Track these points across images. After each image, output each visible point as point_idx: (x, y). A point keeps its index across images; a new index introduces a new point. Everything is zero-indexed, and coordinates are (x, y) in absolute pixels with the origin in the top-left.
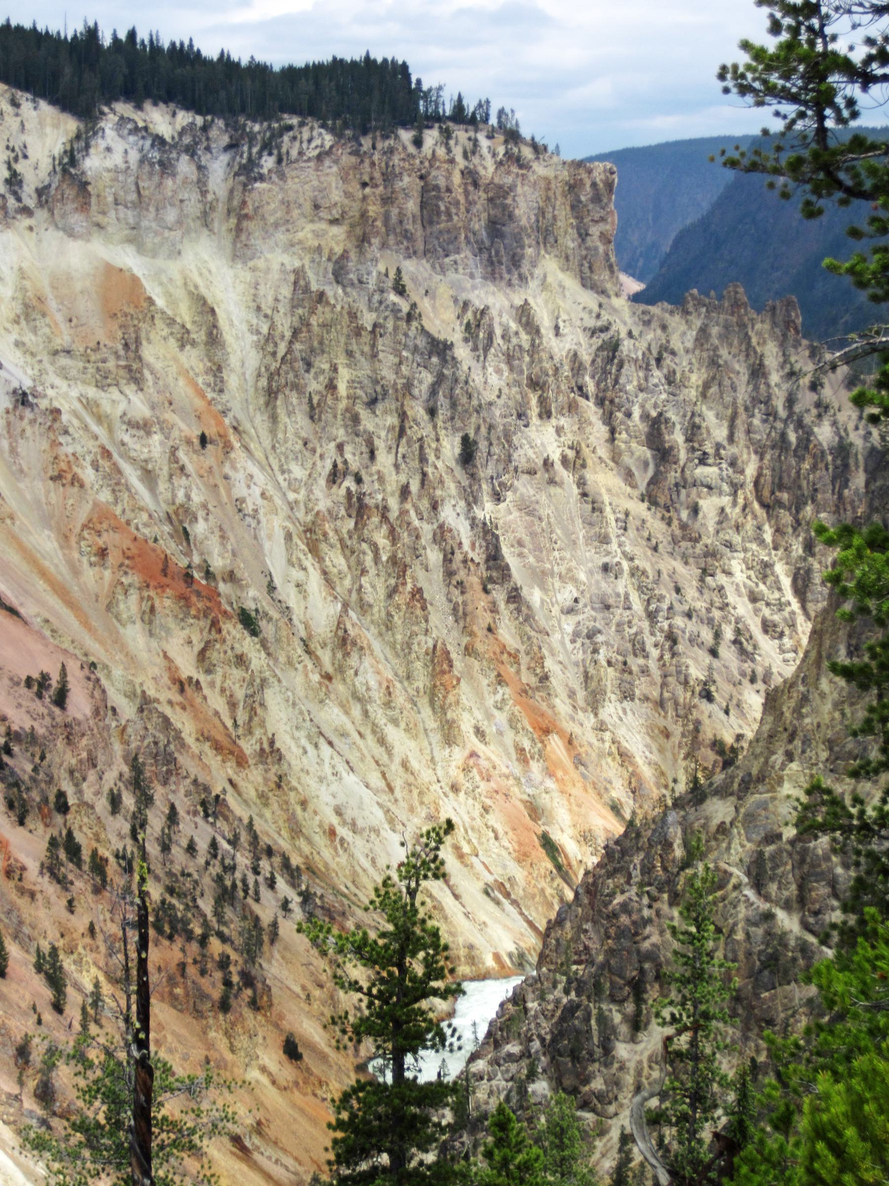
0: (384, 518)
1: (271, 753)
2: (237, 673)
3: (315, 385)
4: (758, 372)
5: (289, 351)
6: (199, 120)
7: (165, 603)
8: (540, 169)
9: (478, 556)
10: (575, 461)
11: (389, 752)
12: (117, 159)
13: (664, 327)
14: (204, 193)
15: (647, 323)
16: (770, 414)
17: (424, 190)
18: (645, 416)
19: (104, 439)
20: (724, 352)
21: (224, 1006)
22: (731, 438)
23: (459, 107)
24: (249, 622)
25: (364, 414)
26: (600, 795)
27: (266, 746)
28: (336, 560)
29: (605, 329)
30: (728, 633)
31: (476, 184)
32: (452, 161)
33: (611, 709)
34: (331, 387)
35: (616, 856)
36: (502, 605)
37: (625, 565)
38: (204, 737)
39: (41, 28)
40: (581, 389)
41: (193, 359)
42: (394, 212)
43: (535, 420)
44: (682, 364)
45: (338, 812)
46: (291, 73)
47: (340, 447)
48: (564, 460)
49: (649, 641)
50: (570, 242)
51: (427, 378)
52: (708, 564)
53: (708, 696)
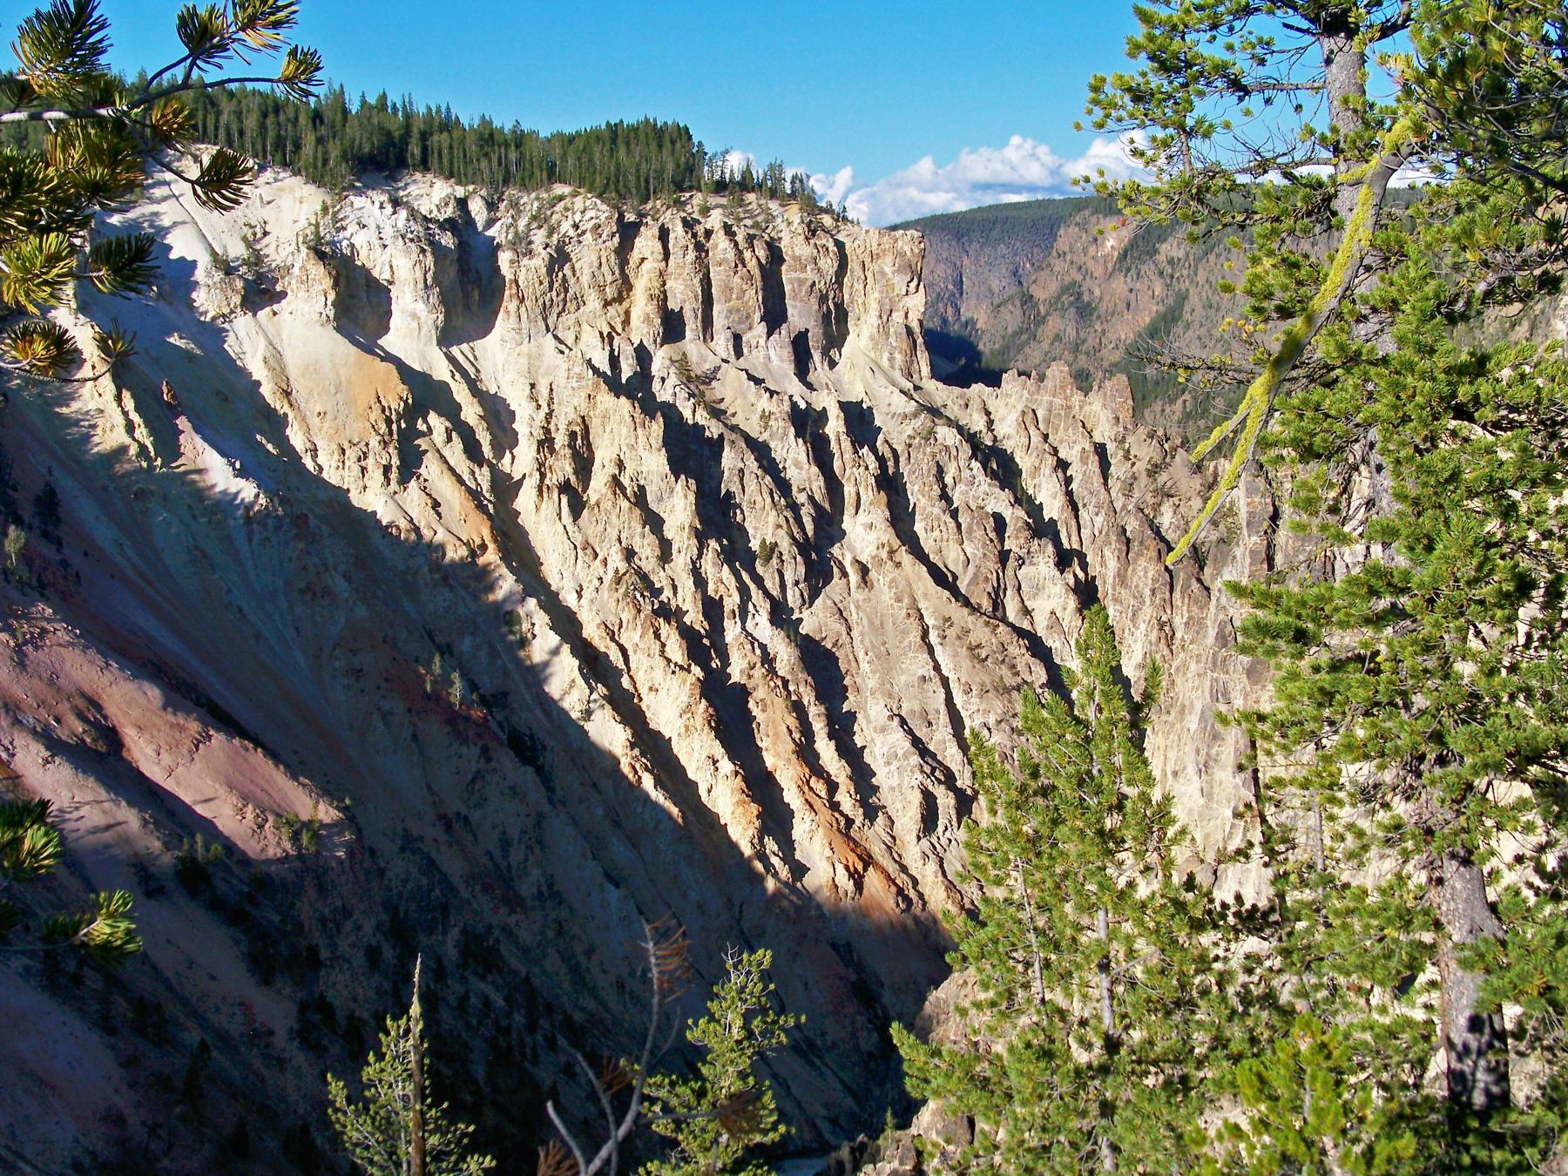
1: (551, 894)
23: (747, 173)
27: (544, 888)
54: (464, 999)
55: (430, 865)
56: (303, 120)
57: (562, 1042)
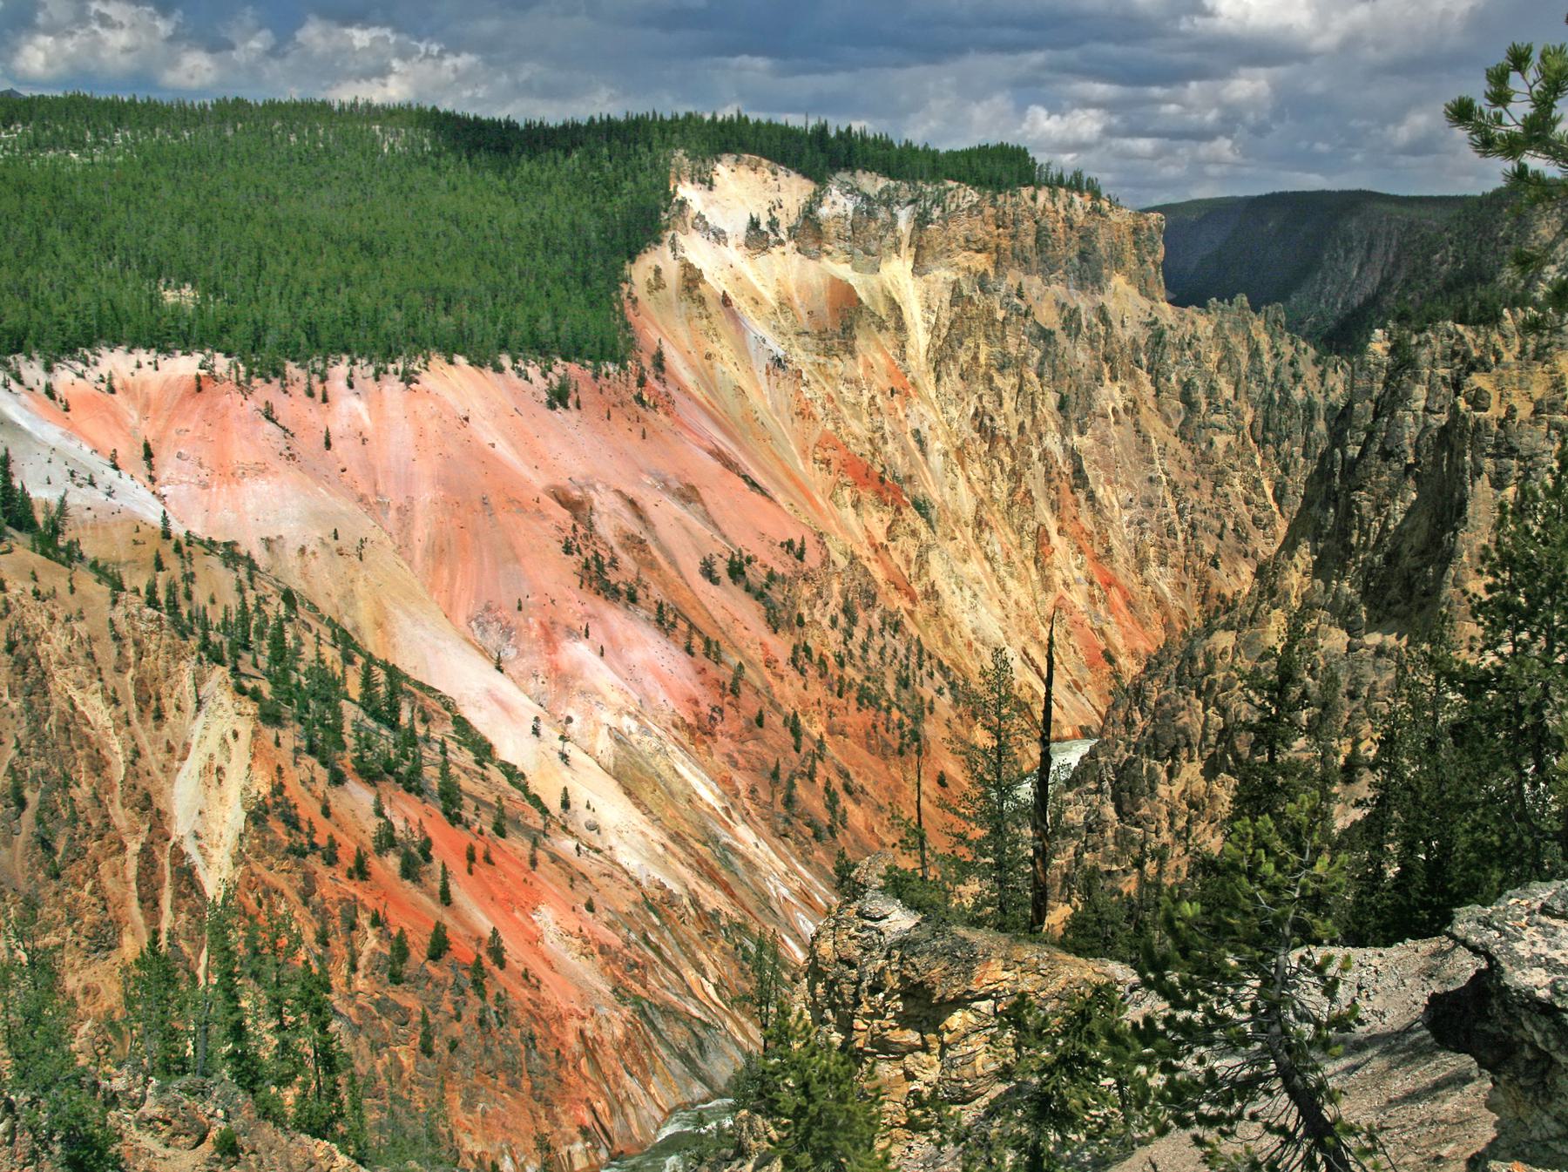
0: (1008, 444)
2: (912, 541)
3: (964, 357)
4: (1255, 354)
5: (949, 334)
6: (892, 183)
7: (868, 495)
8: (1114, 217)
9: (1067, 470)
10: (1132, 409)
11: (1008, 596)
12: (839, 209)
13: (1193, 323)
14: (894, 231)
16: (1262, 381)
17: (1038, 232)
18: (1179, 381)
19: (828, 389)
20: (1233, 340)
21: (901, 752)
22: (1236, 397)
23: (1061, 178)
24: (921, 507)
25: (996, 377)
28: (976, 470)
29: (1155, 322)
30: (1230, 526)
31: (1071, 227)
32: (1057, 212)
33: (1153, 570)
34: (975, 358)
35: (1152, 666)
36: (1082, 501)
37: (1164, 478)
38: (889, 581)
40: (1138, 363)
42: (1018, 245)
43: (1107, 382)
44: (1202, 347)
45: (974, 632)
46: (953, 155)
47: (980, 398)
48: (1126, 409)
49: (1178, 528)
50: (1132, 264)
51: (1038, 353)
52: (1219, 478)
53: (1216, 566)
54: (883, 648)
55: (866, 572)
56: (805, 142)
57: (936, 675)
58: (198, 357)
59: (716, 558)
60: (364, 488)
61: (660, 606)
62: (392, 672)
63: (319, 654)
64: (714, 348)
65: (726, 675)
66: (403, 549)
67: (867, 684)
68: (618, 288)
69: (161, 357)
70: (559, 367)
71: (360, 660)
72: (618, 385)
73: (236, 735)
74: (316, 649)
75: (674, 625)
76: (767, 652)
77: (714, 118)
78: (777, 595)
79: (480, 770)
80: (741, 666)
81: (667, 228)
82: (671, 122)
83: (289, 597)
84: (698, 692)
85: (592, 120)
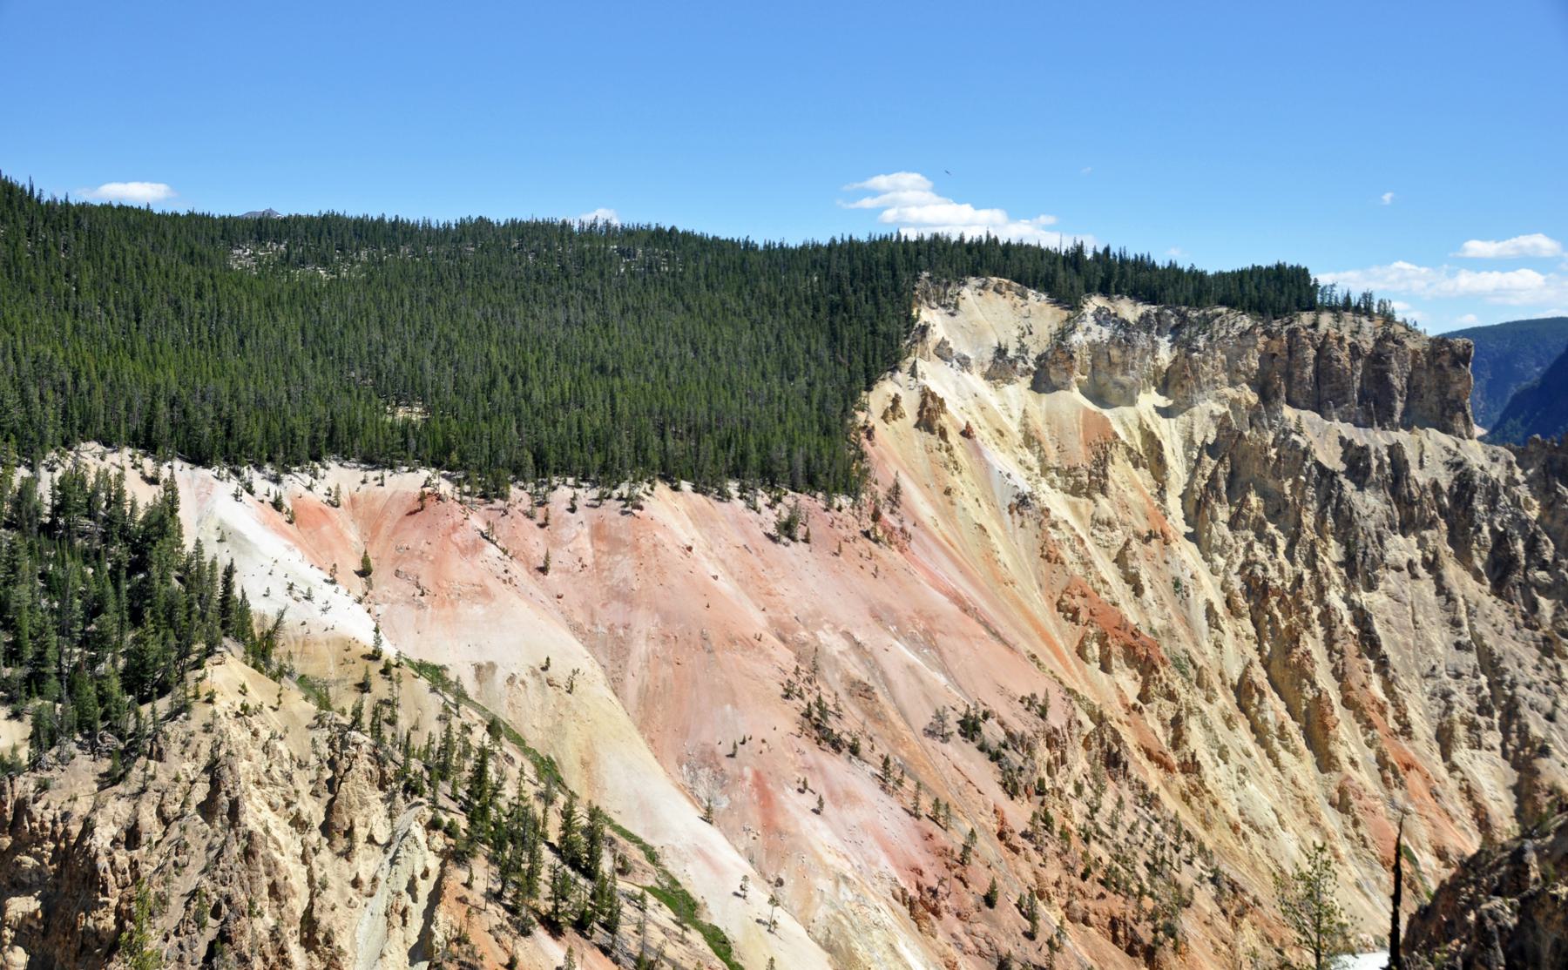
2: (1169, 704)
6: (1154, 309)
15: (1495, 460)
18: (1493, 531)
23: (1348, 298)
26: (1452, 821)
27: (1189, 759)
33: (1461, 754)
39: (1043, 246)
41: (1143, 477)
45: (1241, 813)
46: (1221, 276)
55: (1117, 738)
56: (1060, 263)
58: (424, 473)
59: (949, 712)
60: (580, 617)
61: (886, 762)
62: (594, 814)
63: (520, 790)
64: (954, 481)
65: (955, 840)
66: (616, 685)
67: (1115, 864)
68: (854, 416)
69: (387, 473)
70: (790, 499)
71: (562, 799)
72: (851, 519)
73: (425, 875)
74: (515, 782)
75: (900, 783)
76: (1003, 822)
77: (962, 239)
78: (1015, 758)
79: (679, 930)
80: (972, 833)
81: (909, 354)
82: (916, 243)
83: (494, 728)
84: (922, 860)
85: (833, 240)
